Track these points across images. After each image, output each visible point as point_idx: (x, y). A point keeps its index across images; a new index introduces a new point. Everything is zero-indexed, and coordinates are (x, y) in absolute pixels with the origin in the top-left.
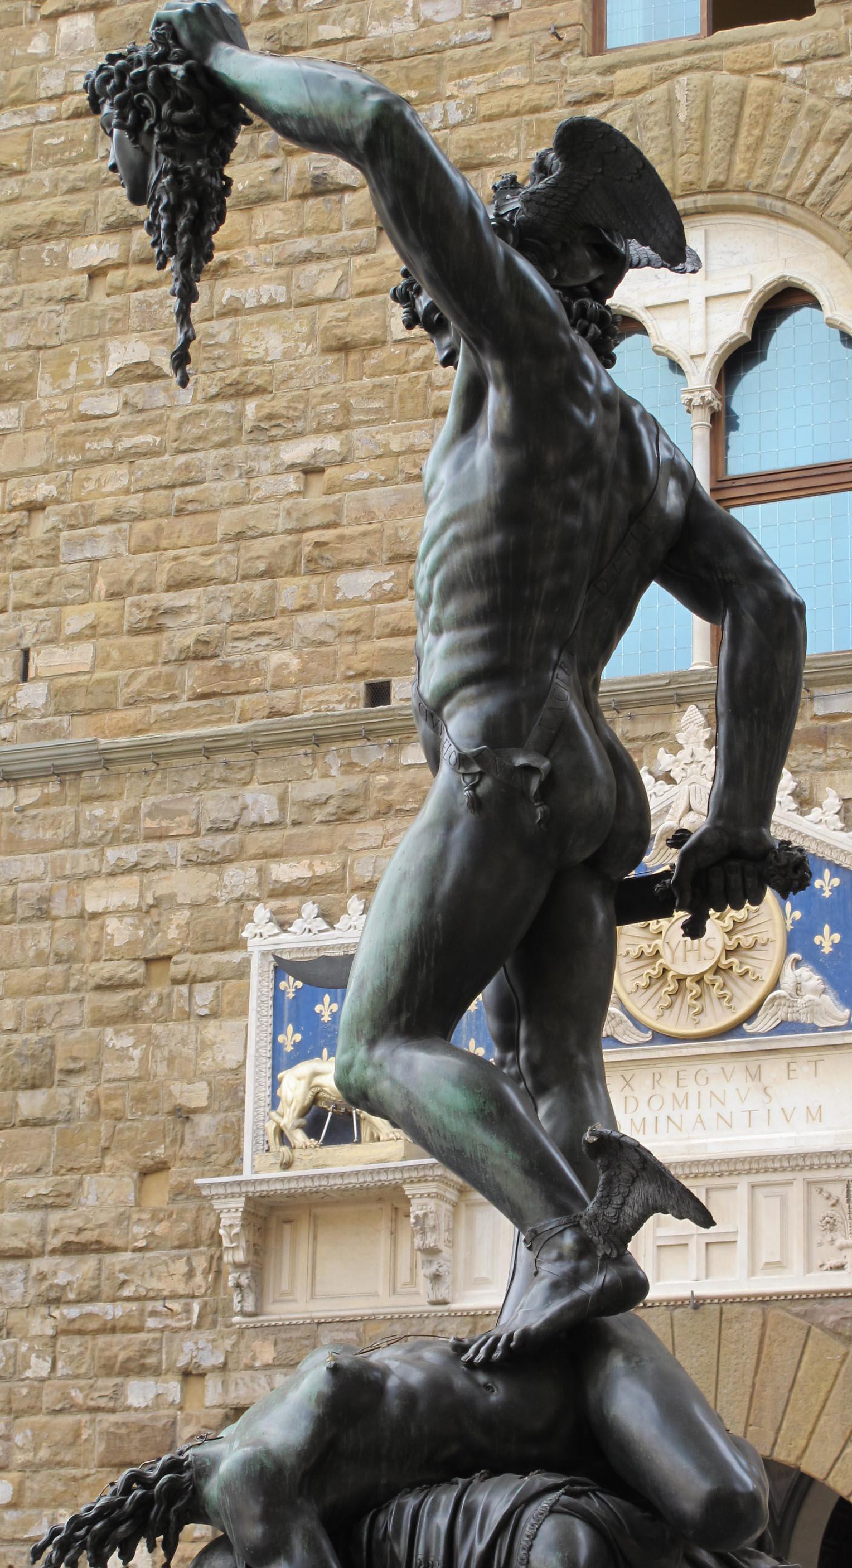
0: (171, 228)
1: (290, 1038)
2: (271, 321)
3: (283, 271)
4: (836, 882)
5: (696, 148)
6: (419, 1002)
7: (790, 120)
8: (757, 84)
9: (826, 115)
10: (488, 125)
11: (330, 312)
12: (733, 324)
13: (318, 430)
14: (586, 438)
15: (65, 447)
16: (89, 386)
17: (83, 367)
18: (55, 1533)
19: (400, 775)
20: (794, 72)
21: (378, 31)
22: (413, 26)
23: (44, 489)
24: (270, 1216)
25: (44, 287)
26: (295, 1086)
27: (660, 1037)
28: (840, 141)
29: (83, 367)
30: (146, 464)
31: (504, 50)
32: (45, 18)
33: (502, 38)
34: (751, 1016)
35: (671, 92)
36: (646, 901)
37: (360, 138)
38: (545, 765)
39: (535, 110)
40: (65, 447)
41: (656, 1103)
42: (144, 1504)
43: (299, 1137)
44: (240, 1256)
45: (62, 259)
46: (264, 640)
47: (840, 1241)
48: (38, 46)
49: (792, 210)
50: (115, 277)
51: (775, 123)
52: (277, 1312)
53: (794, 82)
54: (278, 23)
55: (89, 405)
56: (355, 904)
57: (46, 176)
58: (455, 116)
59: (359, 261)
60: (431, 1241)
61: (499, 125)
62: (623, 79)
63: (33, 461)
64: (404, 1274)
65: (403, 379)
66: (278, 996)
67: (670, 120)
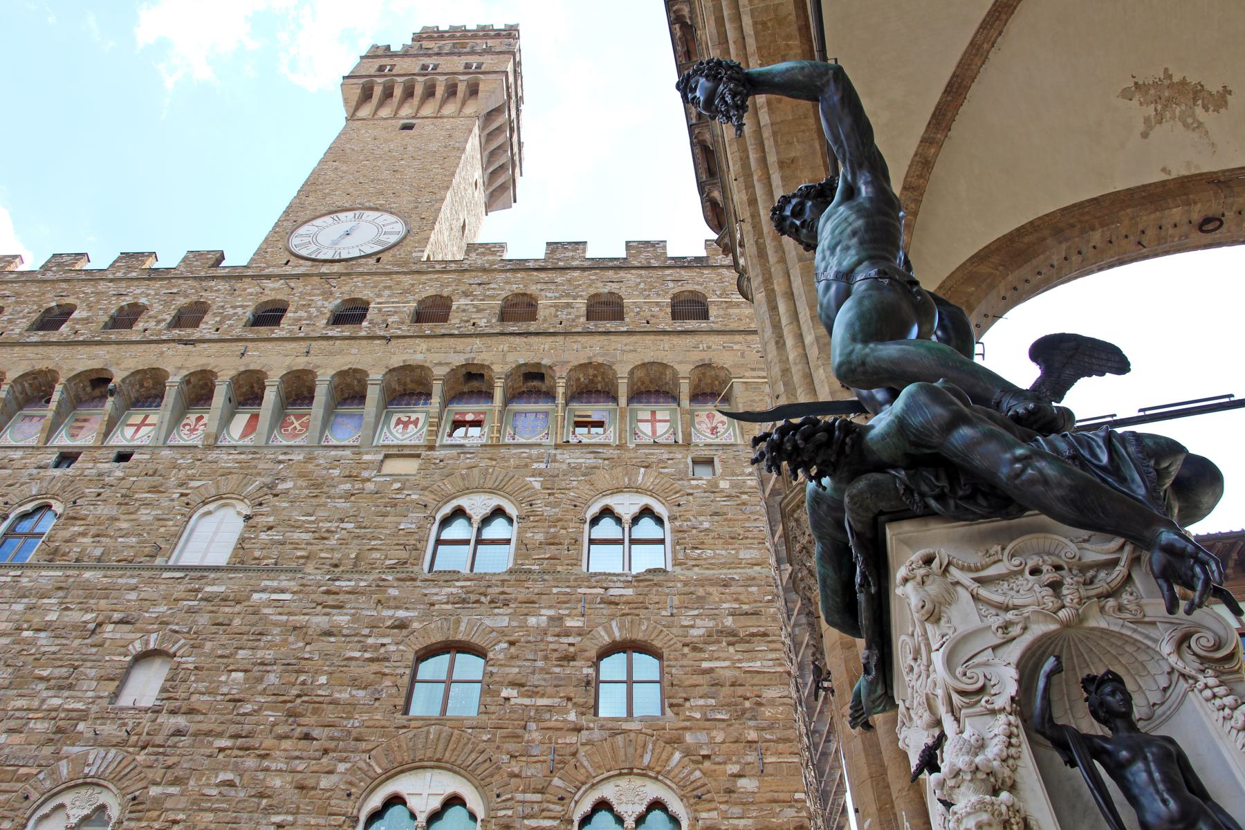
8: (456, 732)
11: (300, 775)
12: (436, 803)
13: (287, 813)
15: (193, 804)
16: (208, 785)
17: (208, 778)
21: (337, 695)
23: (181, 816)
25: (202, 751)
29: (208, 778)
30: (221, 814)
33: (377, 704)
40: (193, 804)
45: (212, 743)
48: (223, 678)
50: (228, 752)
51: (461, 745)
55: (206, 791)
57: (213, 717)
62: (413, 724)
63: (180, 806)
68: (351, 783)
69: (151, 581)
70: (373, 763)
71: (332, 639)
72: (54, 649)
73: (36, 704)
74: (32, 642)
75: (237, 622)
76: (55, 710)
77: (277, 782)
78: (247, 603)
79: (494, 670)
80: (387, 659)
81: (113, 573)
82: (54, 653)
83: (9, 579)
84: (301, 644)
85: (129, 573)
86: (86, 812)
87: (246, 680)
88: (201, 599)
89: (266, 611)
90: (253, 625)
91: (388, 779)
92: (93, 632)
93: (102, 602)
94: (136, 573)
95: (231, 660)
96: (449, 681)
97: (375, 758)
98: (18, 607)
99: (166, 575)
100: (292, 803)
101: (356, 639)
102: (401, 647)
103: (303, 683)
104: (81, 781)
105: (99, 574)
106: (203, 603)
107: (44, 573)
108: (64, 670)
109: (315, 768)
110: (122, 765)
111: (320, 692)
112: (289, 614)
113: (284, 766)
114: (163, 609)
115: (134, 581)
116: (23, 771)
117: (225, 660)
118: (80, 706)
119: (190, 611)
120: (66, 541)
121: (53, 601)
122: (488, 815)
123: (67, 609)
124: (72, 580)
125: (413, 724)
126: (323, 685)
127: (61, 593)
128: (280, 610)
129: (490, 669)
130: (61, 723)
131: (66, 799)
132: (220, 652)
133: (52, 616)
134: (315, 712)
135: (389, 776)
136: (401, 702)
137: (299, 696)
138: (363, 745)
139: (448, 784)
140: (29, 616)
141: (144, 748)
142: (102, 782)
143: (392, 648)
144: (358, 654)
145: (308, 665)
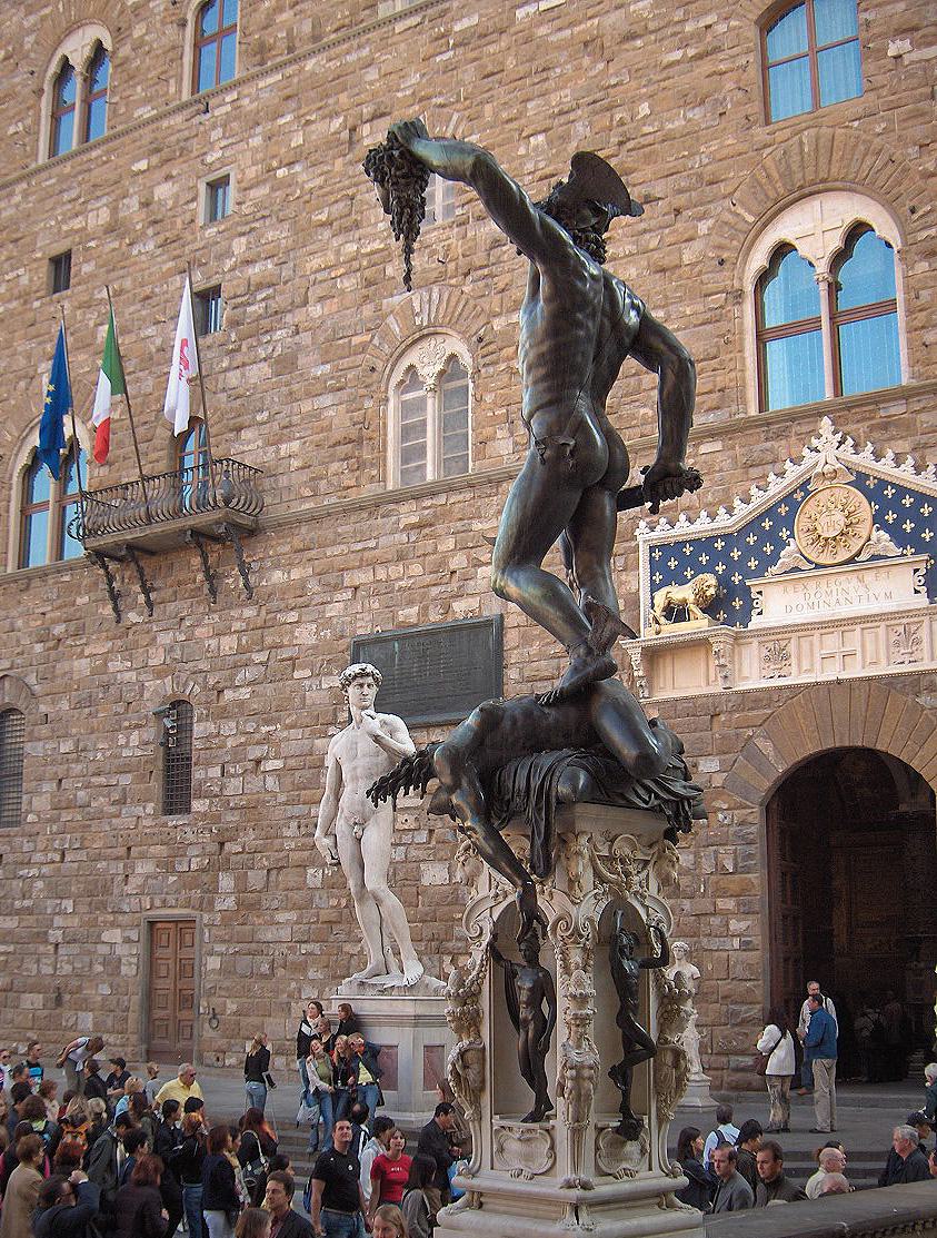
0: (400, 222)
1: (658, 578)
2: (630, 262)
3: (634, 238)
4: (894, 491)
5: (814, 163)
6: (524, 549)
7: (856, 146)
9: (871, 142)
10: (720, 163)
11: (656, 255)
12: (836, 242)
14: (584, 295)
18: (375, 784)
19: (698, 459)
20: (856, 124)
22: (684, 123)
24: (653, 655)
26: (660, 598)
27: (818, 566)
28: (878, 153)
31: (725, 129)
32: (524, 138)
34: (859, 554)
35: (800, 139)
36: (630, 499)
37: (468, 173)
38: (572, 443)
39: (740, 154)
41: (818, 595)
42: (410, 771)
43: (662, 620)
44: (641, 673)
46: (637, 403)
47: (903, 651)
48: (522, 151)
49: (859, 188)
52: (659, 696)
53: (856, 129)
54: (625, 128)
56: (682, 517)
58: (706, 161)
59: (667, 231)
60: (722, 661)
61: (725, 162)
64: (712, 678)
65: (690, 281)
66: (652, 559)
67: (802, 151)
68: (720, 247)
69: (384, 45)
70: (740, 210)
71: (639, 43)
72: (319, 181)
73: (331, 257)
74: (290, 182)
75: (510, 62)
76: (355, 259)
77: (633, 272)
78: (513, 30)
79: (869, 16)
80: (717, 50)
81: (338, 50)
82: (321, 187)
83: (229, 108)
84: (601, 66)
85: (355, 43)
86: (439, 367)
87: (550, 142)
88: (455, 46)
89: (542, 31)
90: (532, 60)
91: (765, 225)
92: (351, 142)
93: (343, 98)
94: (363, 39)
95: (523, 121)
96: (815, 51)
97: (743, 204)
98: (256, 141)
99: (399, 27)
100: (657, 293)
101: (669, 31)
102: (733, 23)
103: (622, 123)
104: (417, 336)
105: (322, 58)
106: (460, 50)
107: (261, 84)
108: (341, 205)
109: (669, 240)
110: (452, 304)
111: (647, 129)
112: (571, 25)
113: (634, 249)
114: (415, 79)
115: (365, 52)
116: (356, 340)
117: (514, 125)
118: (378, 245)
119: (449, 68)
120: (265, 28)
121: (289, 118)
122: (905, 243)
123: (308, 123)
124: (295, 80)
125: (780, 136)
126: (646, 116)
127: (292, 104)
128: (557, 23)
129: (864, 16)
130: (367, 273)
131: (412, 358)
132: (505, 115)
133: (297, 140)
134: (648, 159)
135: (767, 220)
136: (755, 108)
137: (621, 143)
138: (723, 188)
139: (841, 210)
140: (273, 149)
141: (466, 275)
142: (439, 330)
143: (722, 28)
144: (677, 55)
145: (616, 95)
